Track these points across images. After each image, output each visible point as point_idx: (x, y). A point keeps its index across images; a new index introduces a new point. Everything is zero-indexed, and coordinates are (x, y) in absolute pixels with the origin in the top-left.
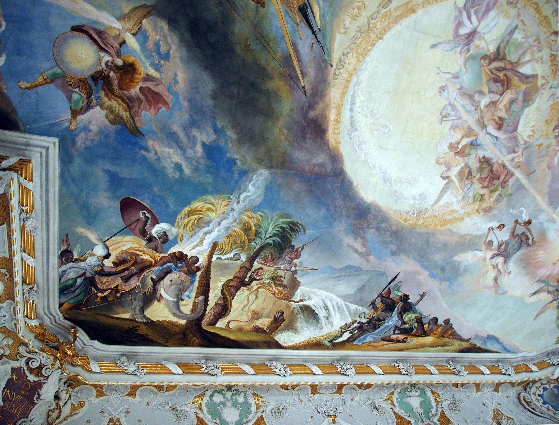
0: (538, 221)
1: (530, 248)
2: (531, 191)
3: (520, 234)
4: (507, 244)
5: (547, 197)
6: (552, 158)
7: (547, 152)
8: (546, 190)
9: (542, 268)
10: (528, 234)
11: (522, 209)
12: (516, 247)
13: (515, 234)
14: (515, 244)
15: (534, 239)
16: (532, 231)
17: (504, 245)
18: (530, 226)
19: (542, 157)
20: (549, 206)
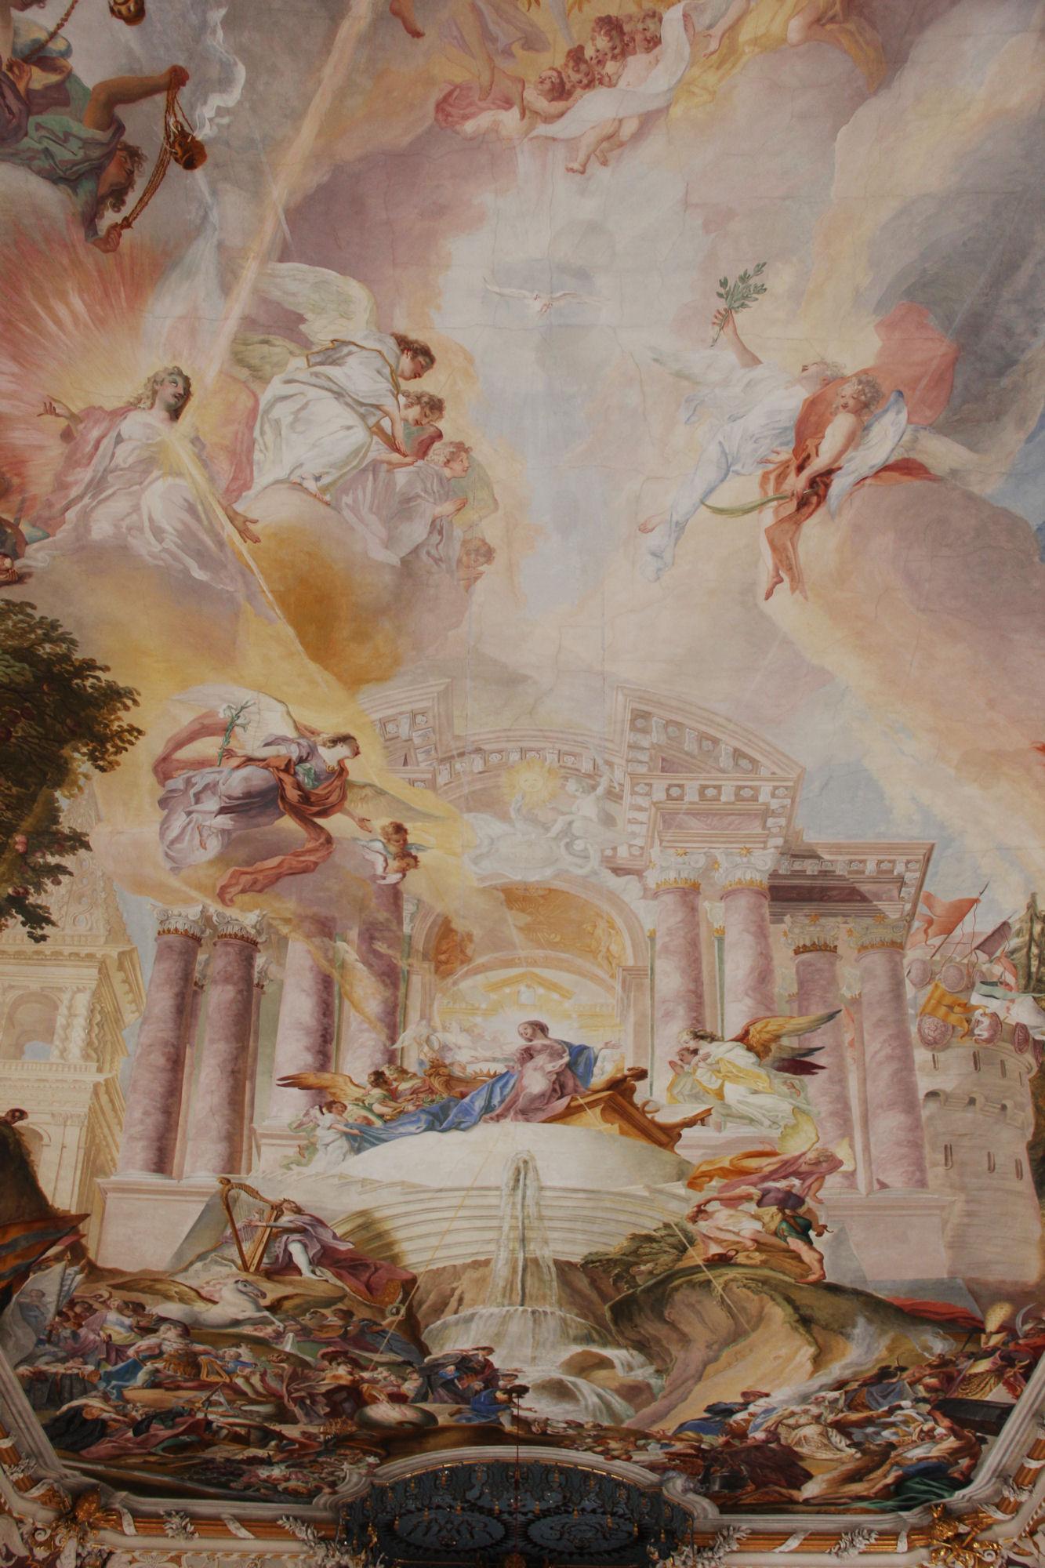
0: (209, 199)
1: (78, 234)
2: (328, 70)
3: (128, 138)
4: (60, 96)
5: (321, 177)
6: (486, 93)
7: (508, 53)
8: (348, 150)
9: (14, 358)
10: (140, 184)
11: (241, 73)
12: (63, 154)
13: (120, 111)
14: (74, 144)
15: (126, 232)
16: (157, 200)
17: (54, 78)
18: (175, 168)
19: (487, 36)
20: (287, 212)
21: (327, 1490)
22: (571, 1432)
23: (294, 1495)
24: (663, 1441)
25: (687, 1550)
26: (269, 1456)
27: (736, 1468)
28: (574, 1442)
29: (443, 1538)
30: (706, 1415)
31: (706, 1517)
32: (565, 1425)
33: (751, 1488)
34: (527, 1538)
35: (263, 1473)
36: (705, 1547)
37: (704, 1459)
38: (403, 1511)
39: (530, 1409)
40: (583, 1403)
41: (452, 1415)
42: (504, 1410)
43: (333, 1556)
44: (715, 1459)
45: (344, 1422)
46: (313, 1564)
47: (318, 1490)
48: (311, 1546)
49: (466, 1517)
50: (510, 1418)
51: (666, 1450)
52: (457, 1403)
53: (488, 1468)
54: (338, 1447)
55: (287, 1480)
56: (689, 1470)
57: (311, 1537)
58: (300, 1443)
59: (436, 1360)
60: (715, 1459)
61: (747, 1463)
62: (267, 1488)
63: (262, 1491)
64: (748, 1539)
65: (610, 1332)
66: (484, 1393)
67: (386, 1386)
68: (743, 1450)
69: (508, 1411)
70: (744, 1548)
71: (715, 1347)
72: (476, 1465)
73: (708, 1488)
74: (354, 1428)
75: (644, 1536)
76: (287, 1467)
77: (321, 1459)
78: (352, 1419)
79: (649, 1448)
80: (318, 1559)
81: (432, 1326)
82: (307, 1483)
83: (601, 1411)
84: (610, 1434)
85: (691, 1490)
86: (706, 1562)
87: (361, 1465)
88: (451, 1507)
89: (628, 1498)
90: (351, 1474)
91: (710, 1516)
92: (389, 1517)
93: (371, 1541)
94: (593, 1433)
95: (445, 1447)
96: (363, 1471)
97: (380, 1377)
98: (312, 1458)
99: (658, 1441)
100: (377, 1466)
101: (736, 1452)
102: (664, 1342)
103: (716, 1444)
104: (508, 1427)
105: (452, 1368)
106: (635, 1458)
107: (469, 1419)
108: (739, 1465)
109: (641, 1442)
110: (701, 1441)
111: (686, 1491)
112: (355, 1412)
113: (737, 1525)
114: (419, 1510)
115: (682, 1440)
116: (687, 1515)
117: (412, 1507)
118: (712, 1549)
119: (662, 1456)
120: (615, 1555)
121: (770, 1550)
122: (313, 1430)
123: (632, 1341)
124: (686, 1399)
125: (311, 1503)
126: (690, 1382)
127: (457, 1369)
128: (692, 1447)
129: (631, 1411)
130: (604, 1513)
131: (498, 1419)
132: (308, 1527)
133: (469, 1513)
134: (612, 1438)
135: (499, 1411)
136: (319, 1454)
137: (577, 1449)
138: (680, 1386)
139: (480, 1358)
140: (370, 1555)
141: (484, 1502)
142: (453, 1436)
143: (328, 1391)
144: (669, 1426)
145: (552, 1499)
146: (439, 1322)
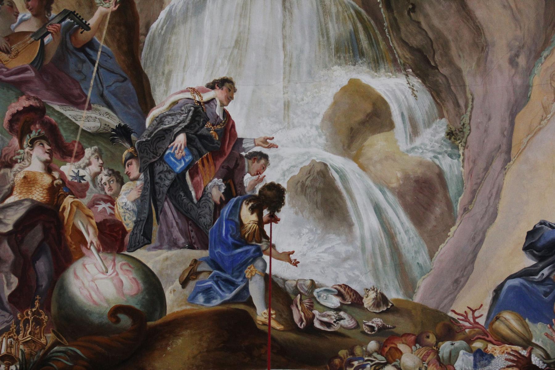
22: (347, 322)
30: (528, 262)
32: (335, 302)
39: (287, 257)
40: (357, 230)
45: (38, 322)
52: (191, 247)
59: (160, 120)
65: (379, 22)
66: (226, 211)
67: (93, 204)
71: (522, 61)
78: (48, 309)
81: (154, 26)
94: (377, 322)
97: (86, 173)
99: (469, 340)
102: (454, 52)
105: (181, 139)
107: (207, 291)
109: (446, 347)
110: (527, 343)
115: (503, 340)
123: (412, 49)
124: (494, 215)
126: (497, 164)
127: (189, 141)
129: (423, 257)
131: (246, 288)
135: (245, 264)
138: (483, 178)
139: (218, 112)
143: (18, 224)
146: (163, 15)
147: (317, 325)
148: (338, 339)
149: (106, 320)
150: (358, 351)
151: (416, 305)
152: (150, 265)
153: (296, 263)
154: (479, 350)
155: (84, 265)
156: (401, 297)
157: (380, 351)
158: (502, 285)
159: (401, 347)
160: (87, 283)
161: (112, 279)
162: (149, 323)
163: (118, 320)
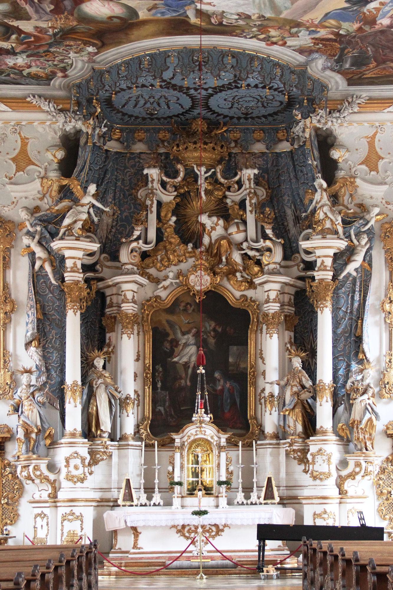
21: (60, 74)
22: (241, 22)
23: (36, 79)
24: (311, 28)
25: (321, 112)
26: (13, 48)
27: (364, 49)
28: (243, 31)
29: (148, 108)
31: (337, 89)
33: (373, 65)
34: (208, 107)
35: (10, 61)
36: (334, 110)
37: (341, 42)
38: (117, 89)
39: (210, 4)
41: (149, 10)
42: (190, 4)
43: (70, 122)
44: (349, 43)
45: (66, 18)
46: (57, 128)
47: (53, 75)
48: (53, 116)
49: (163, 93)
50: (194, 12)
51: (313, 36)
53: (179, 53)
54: (64, 39)
55: (29, 67)
56: (329, 52)
57: (53, 109)
58: (35, 36)
60: (349, 43)
61: (373, 46)
62: (15, 74)
63: (12, 75)
64: (366, 103)
68: (370, 35)
69: (193, 6)
70: (362, 110)
72: (169, 51)
73: (341, 66)
74: (75, 23)
75: (291, 104)
76: (28, 56)
77: (52, 50)
78: (72, 15)
79: (299, 35)
80: (60, 124)
82: (44, 69)
83: (265, 4)
84: (271, 24)
85: (328, 68)
86: (334, 120)
87: (83, 53)
88: (152, 85)
89: (282, 76)
90: (76, 61)
91: (340, 88)
92: (108, 94)
93: (96, 111)
94: (258, 23)
95: (146, 37)
96: (86, 59)
98: (45, 49)
99: (308, 28)
100: (96, 54)
101: (366, 37)
103: (351, 30)
104: (193, 20)
106: (289, 43)
107: (163, 13)
108: (367, 47)
109: (294, 30)
110: (339, 28)
111: (324, 69)
112: (74, 9)
113: (359, 94)
114: (130, 88)
116: (324, 87)
117: (124, 86)
118: (339, 111)
119: (311, 41)
120: (270, 119)
121: (381, 111)
122: (43, 25)
125: (49, 85)
128: (333, 33)
130: (264, 87)
131: (185, 12)
132: (49, 102)
133: (166, 89)
134: (272, 27)
135: (185, 6)
136: (50, 45)
137: (245, 37)
140: (97, 121)
141: (176, 81)
142: (150, 28)
144: (316, 16)
145: (227, 77)
147: (224, 23)
148: (236, 28)
149: (105, 19)
150: (246, 31)
151: (281, 18)
152: (129, 5)
153: (214, 6)
154: (313, 31)
155: (91, 4)
156: (273, 16)
157: (259, 31)
158: (330, 12)
159: (270, 30)
160: (93, 8)
161: (108, 8)
162: (130, 21)
163: (112, 20)
